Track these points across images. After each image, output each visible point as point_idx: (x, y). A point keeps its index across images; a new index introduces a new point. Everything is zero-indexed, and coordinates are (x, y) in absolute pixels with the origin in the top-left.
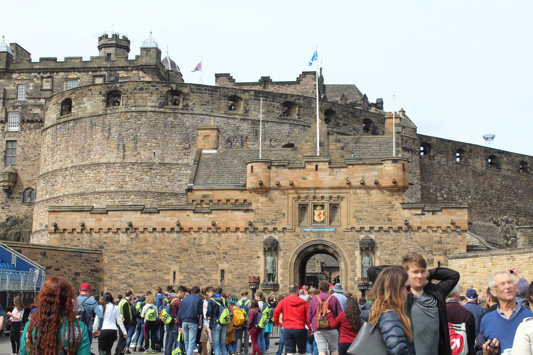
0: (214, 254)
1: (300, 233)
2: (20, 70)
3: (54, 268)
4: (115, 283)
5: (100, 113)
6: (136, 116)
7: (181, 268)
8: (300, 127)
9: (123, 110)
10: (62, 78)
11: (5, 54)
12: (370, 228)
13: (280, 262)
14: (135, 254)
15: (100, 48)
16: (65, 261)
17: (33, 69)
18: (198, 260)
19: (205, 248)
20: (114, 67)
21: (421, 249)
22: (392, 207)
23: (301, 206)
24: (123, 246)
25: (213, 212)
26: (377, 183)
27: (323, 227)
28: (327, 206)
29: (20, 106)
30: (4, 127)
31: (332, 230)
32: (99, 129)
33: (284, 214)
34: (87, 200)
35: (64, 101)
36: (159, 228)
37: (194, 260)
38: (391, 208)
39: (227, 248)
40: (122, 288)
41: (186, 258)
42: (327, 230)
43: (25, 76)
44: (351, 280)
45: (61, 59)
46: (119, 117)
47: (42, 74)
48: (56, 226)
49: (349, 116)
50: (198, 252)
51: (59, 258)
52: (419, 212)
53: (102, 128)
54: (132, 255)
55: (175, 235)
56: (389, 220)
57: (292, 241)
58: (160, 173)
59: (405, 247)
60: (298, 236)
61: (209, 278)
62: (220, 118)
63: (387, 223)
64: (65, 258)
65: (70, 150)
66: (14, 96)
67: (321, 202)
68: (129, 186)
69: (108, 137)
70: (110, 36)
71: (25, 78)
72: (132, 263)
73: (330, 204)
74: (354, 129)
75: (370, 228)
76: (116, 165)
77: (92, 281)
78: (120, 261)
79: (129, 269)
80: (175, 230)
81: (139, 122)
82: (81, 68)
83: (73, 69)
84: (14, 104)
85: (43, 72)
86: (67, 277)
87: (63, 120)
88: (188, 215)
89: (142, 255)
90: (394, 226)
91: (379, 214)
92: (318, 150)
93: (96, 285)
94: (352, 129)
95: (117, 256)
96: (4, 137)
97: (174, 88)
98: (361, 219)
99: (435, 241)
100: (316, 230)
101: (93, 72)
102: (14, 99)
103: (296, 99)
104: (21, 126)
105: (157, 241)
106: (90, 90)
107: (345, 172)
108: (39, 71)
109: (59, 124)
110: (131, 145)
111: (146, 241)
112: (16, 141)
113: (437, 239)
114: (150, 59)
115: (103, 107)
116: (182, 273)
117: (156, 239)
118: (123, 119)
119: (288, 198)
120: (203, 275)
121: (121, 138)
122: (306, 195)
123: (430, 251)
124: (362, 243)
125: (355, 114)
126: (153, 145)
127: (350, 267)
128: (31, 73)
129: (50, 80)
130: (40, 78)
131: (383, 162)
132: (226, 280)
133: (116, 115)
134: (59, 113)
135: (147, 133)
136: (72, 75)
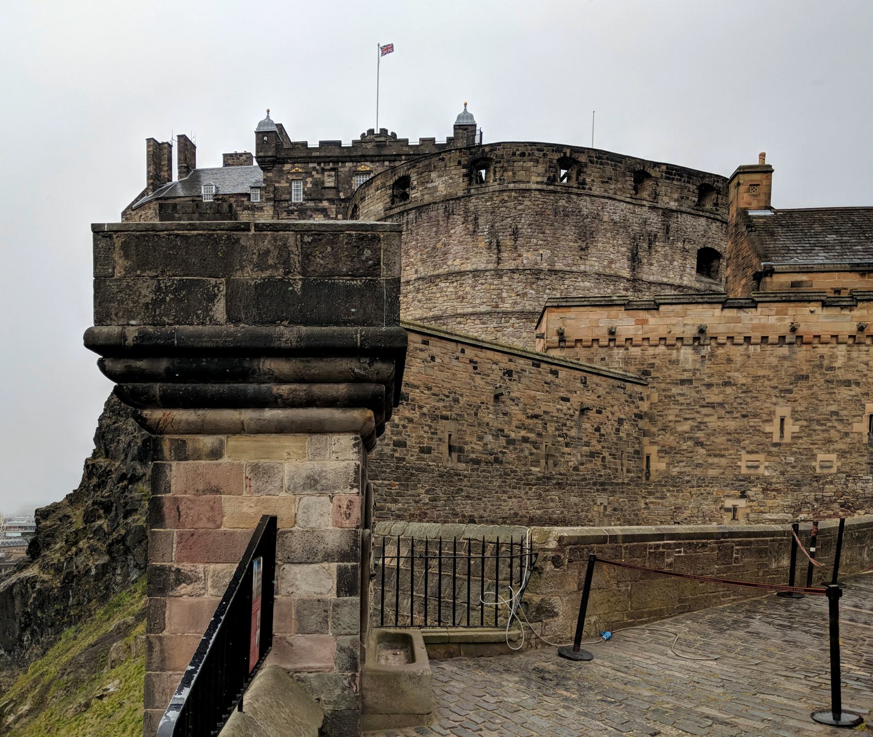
0: (858, 384)
2: (294, 158)
3: (595, 410)
8: (718, 224)
10: (349, 171)
14: (709, 386)
17: (311, 157)
18: (828, 396)
19: (841, 375)
24: (685, 370)
32: (458, 219)
41: (805, 392)
47: (322, 165)
48: (561, 334)
50: (827, 381)
51: (601, 391)
58: (549, 284)
64: (608, 390)
69: (474, 232)
71: (300, 170)
82: (375, 156)
83: (364, 158)
85: (325, 163)
87: (397, 210)
89: (722, 388)
95: (675, 390)
101: (390, 161)
108: (318, 160)
109: (391, 216)
110: (508, 242)
111: (729, 361)
121: (493, 233)
126: (540, 242)
128: (308, 163)
129: (333, 173)
130: (320, 171)
134: (388, 200)
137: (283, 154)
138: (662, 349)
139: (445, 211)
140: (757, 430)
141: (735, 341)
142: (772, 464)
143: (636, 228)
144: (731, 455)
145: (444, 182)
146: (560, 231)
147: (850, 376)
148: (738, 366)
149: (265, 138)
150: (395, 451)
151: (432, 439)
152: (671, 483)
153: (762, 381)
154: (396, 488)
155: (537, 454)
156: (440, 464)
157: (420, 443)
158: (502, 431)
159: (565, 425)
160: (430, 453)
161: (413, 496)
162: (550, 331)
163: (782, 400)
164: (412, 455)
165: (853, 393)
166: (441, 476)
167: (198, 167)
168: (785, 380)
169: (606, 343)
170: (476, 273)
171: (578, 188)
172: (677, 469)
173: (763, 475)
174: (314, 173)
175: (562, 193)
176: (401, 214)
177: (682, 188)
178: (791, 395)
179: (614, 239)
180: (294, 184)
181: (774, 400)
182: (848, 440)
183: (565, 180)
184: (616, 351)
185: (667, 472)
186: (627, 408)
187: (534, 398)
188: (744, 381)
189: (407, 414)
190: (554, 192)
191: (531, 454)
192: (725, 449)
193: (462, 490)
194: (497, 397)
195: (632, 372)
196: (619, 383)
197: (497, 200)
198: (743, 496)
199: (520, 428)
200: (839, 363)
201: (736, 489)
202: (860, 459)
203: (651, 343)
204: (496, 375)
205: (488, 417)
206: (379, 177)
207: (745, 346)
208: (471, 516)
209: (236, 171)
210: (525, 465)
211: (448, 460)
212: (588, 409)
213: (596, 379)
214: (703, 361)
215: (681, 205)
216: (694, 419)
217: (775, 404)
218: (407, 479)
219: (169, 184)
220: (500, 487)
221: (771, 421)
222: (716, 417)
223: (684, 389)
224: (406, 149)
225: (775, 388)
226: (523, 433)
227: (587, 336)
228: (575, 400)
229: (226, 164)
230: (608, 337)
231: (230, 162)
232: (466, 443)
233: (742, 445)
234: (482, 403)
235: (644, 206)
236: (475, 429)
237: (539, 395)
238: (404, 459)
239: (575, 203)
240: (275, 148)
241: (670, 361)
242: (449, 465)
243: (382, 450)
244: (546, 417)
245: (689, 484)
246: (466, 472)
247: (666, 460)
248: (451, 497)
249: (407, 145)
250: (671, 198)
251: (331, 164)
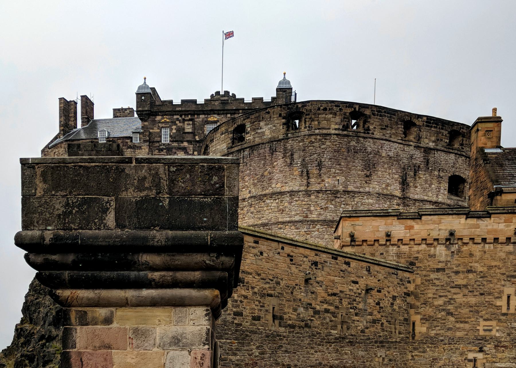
2: (164, 112)
8: (463, 158)
10: (203, 121)
14: (457, 273)
24: (440, 262)
32: (280, 155)
43: (168, 119)
47: (183, 117)
48: (352, 236)
51: (380, 276)
64: (385, 276)
82: (221, 110)
83: (213, 112)
85: (185, 115)
87: (236, 149)
89: (466, 275)
101: (231, 114)
110: (314, 171)
128: (173, 115)
134: (230, 141)
135: (331, 159)
136: (212, 118)
137: (155, 109)
138: (423, 246)
139: (270, 149)
140: (491, 304)
141: (476, 241)
142: (501, 328)
143: (405, 161)
144: (472, 321)
145: (269, 129)
146: (351, 163)
148: (478, 258)
149: (143, 98)
150: (234, 319)
151: (261, 310)
152: (430, 341)
153: (494, 269)
154: (235, 345)
155: (335, 321)
156: (267, 328)
157: (252, 313)
158: (311, 304)
159: (355, 300)
160: (259, 320)
161: (248, 350)
162: (344, 234)
163: (508, 283)
164: (247, 322)
166: (267, 336)
167: (95, 118)
168: (511, 269)
169: (384, 243)
170: (292, 193)
171: (364, 133)
172: (434, 332)
173: (495, 336)
175: (353, 136)
176: (239, 151)
177: (438, 133)
179: (390, 169)
180: (163, 130)
183: (355, 128)
184: (391, 248)
185: (426, 334)
186: (399, 289)
187: (333, 281)
188: (481, 269)
189: (243, 293)
190: (347, 136)
191: (331, 321)
192: (468, 318)
193: (282, 346)
194: (307, 281)
195: (403, 263)
197: (307, 142)
198: (481, 350)
199: (323, 303)
201: (476, 346)
203: (416, 242)
204: (307, 265)
205: (300, 295)
206: (224, 125)
207: (482, 245)
208: (288, 365)
209: (122, 121)
210: (327, 329)
211: (272, 326)
212: (371, 289)
213: (377, 268)
214: (452, 255)
215: (437, 145)
216: (446, 296)
217: (504, 286)
218: (243, 339)
219: (75, 130)
220: (309, 344)
221: (501, 297)
222: (462, 294)
224: (242, 105)
226: (325, 306)
227: (370, 237)
228: (362, 282)
229: (115, 116)
230: (385, 238)
231: (118, 114)
232: (285, 313)
233: (480, 314)
234: (296, 285)
235: (411, 145)
236: (292, 303)
237: (337, 279)
238: (241, 325)
239: (362, 143)
240: (149, 105)
241: (429, 255)
242: (273, 329)
243: (226, 318)
244: (342, 295)
245: (443, 342)
246: (285, 334)
247: (427, 325)
248: (274, 352)
249: (244, 103)
250: (430, 140)
251: (189, 116)
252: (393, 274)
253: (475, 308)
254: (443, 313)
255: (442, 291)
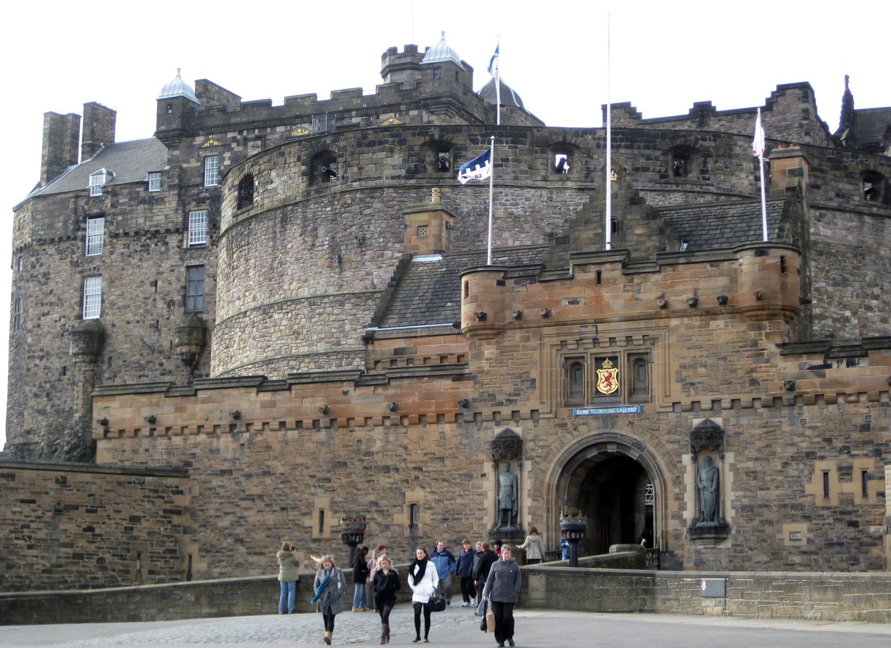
1: (567, 421)
2: (207, 128)
4: (212, 535)
5: (299, 199)
6: (361, 200)
7: (333, 502)
9: (339, 188)
11: (180, 101)
12: (713, 401)
13: (527, 484)
14: (248, 476)
15: (384, 74)
16: (108, 494)
18: (366, 485)
20: (375, 108)
21: (824, 444)
22: (759, 354)
23: (571, 362)
24: (225, 460)
25: (393, 383)
26: (724, 301)
27: (614, 404)
28: (623, 360)
29: (208, 198)
30: (181, 241)
31: (633, 410)
32: (294, 230)
33: (533, 381)
34: (276, 373)
35: (241, 182)
36: (291, 421)
37: (360, 486)
38: (757, 355)
39: (421, 458)
40: (225, 545)
41: (344, 480)
42: (624, 410)
44: (673, 517)
45: (278, 102)
46: (331, 204)
47: (245, 133)
49: (826, 166)
50: (365, 468)
51: (94, 489)
52: (818, 361)
53: (302, 228)
54: (242, 479)
55: (322, 435)
56: (753, 382)
57: (551, 439)
59: (790, 442)
60: (563, 426)
61: (387, 521)
62: (533, 191)
63: (748, 389)
64: (109, 487)
65: (251, 275)
66: (198, 180)
67: (609, 350)
68: (350, 341)
69: (313, 245)
70: (401, 50)
71: (216, 143)
72: (242, 495)
73: (629, 355)
74: (838, 195)
75: (713, 401)
76: (326, 300)
77: (168, 532)
78: (221, 491)
79: (238, 506)
80: (322, 425)
81: (367, 211)
84: (198, 195)
85: (248, 130)
86: (114, 526)
88: (345, 393)
90: (763, 396)
91: (732, 371)
92: (608, 238)
93: (177, 541)
94: (832, 194)
95: (216, 482)
96: (182, 259)
97: (436, 136)
98: (692, 384)
99: (855, 426)
100: (601, 411)
102: (197, 186)
103: (697, 140)
104: (211, 237)
105: (290, 448)
106: (282, 154)
107: (656, 284)
111: (268, 448)
112: (202, 266)
113: (860, 421)
114: (440, 85)
115: (303, 186)
116: (336, 512)
117: (287, 443)
118: (338, 207)
119: (541, 346)
120: (375, 516)
121: (334, 247)
122: (577, 337)
123: (845, 448)
124: (696, 434)
125: (840, 162)
127: (672, 490)
129: (259, 143)
130: (241, 142)
131: (738, 256)
132: (420, 525)
133: (326, 200)
135: (384, 232)
147: (389, 462)
153: (299, 469)
165: (391, 480)
174: (234, 145)
178: (329, 485)
181: (313, 490)
182: (389, 534)
186: (148, 506)
195: (175, 461)
196: (133, 478)
200: (378, 446)
202: (401, 555)
217: (313, 495)
223: (225, 480)
225: (313, 477)
241: (210, 450)
251: (257, 132)
252: (129, 483)
253: (274, 530)
254: (230, 540)
255: (228, 505)
